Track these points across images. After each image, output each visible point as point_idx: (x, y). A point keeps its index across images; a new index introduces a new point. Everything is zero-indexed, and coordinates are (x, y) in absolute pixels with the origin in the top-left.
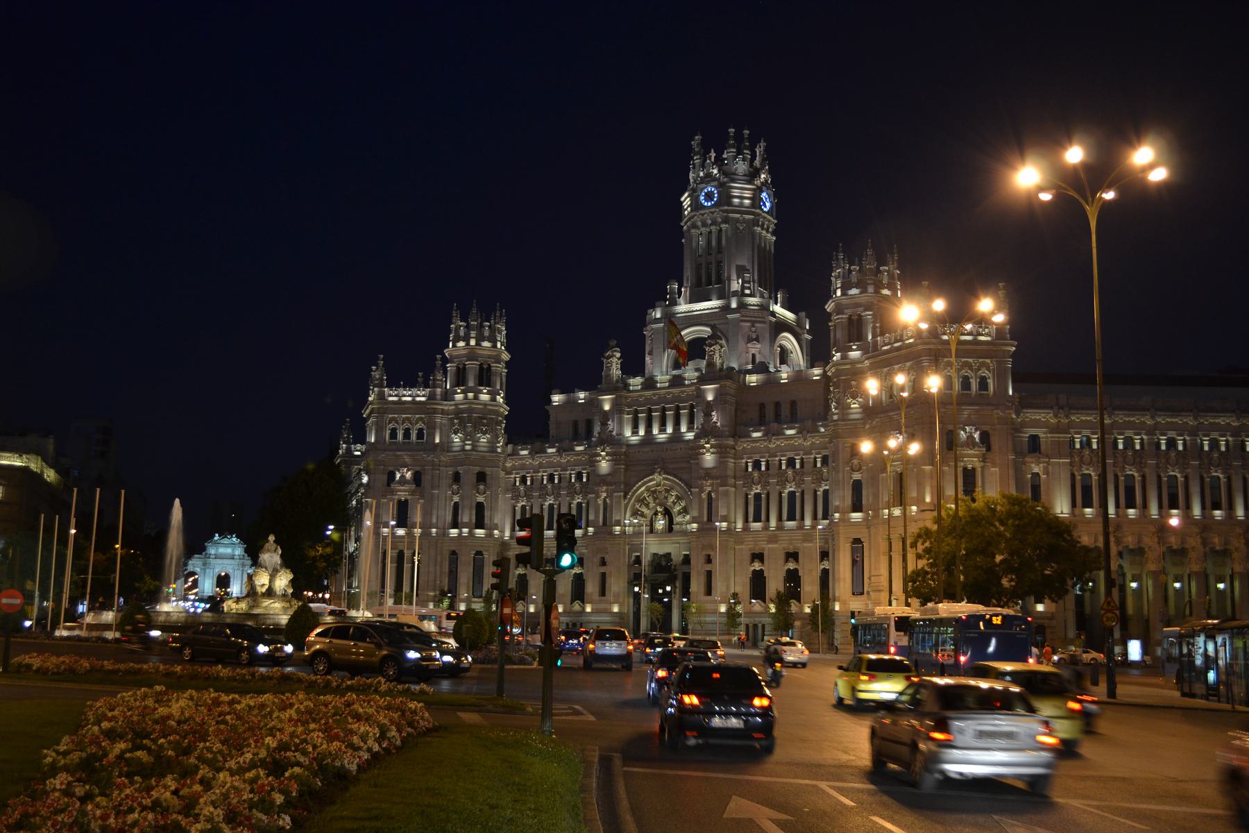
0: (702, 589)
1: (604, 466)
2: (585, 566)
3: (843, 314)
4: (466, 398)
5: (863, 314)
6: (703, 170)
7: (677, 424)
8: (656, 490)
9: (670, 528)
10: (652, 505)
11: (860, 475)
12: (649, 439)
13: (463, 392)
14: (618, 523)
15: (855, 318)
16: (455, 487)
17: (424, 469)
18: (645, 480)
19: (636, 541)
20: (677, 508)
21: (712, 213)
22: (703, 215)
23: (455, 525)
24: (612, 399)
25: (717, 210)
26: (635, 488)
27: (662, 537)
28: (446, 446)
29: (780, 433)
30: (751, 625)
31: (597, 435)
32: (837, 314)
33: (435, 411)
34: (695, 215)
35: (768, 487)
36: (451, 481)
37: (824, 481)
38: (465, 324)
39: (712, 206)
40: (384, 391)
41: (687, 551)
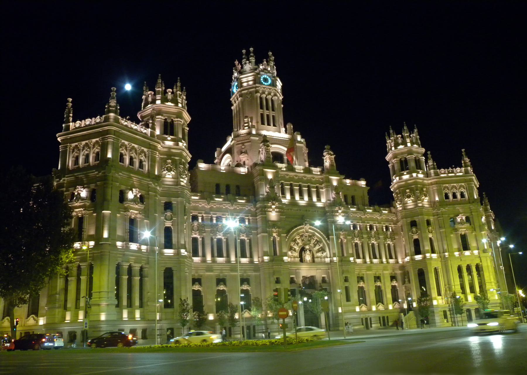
0: (344, 297)
1: (273, 215)
2: (251, 284)
4: (178, 145)
5: (408, 157)
6: (262, 66)
7: (310, 196)
9: (313, 261)
11: (432, 235)
12: (293, 203)
13: (176, 141)
14: (286, 254)
16: (169, 214)
17: (149, 194)
18: (298, 228)
19: (294, 267)
20: (317, 247)
21: (270, 89)
22: (264, 88)
23: (168, 244)
24: (273, 173)
25: (273, 88)
26: (291, 232)
27: (311, 265)
28: (158, 178)
29: (364, 210)
30: (364, 319)
31: (265, 194)
33: (155, 148)
34: (260, 87)
35: (363, 240)
36: (163, 208)
37: (388, 238)
38: (153, 93)
39: (267, 85)
40: (119, 119)
41: (324, 274)
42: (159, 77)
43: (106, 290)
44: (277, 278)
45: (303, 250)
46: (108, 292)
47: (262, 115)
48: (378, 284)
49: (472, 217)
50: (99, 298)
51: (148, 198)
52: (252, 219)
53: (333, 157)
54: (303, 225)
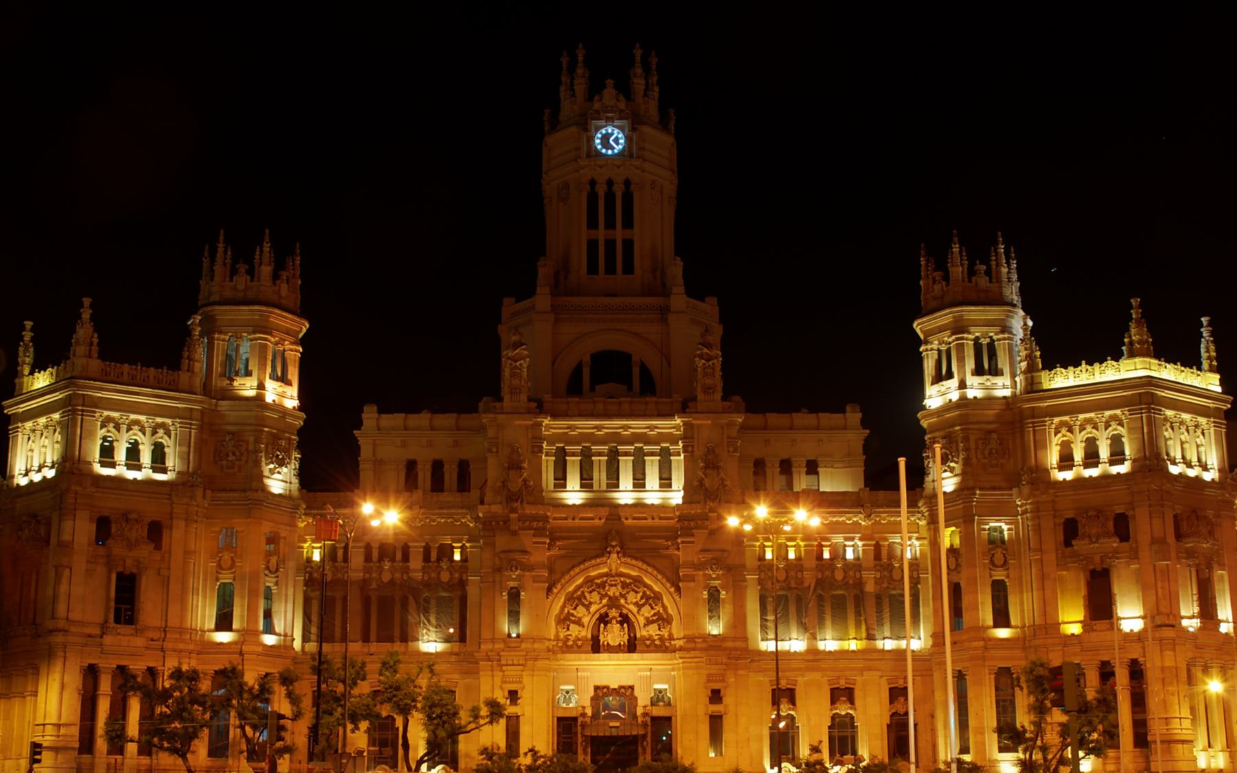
3: (969, 333)
8: (606, 582)
10: (593, 608)
15: (985, 341)
32: (953, 334)
42: (221, 238)
43: (54, 721)
44: (511, 692)
45: (603, 619)
46: (60, 725)
47: (592, 245)
48: (843, 710)
49: (1134, 517)
50: (43, 736)
51: (171, 528)
52: (471, 547)
53: (718, 362)
54: (602, 555)
